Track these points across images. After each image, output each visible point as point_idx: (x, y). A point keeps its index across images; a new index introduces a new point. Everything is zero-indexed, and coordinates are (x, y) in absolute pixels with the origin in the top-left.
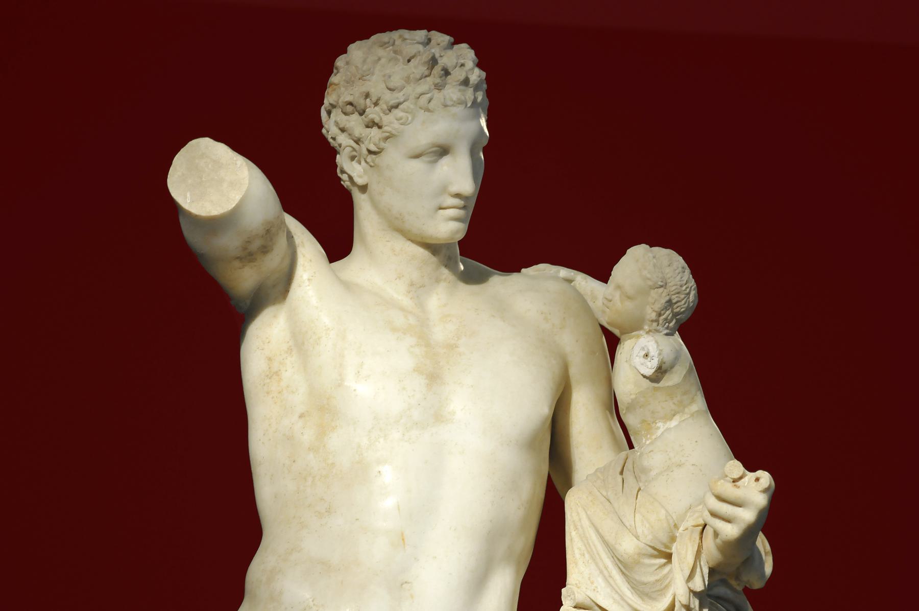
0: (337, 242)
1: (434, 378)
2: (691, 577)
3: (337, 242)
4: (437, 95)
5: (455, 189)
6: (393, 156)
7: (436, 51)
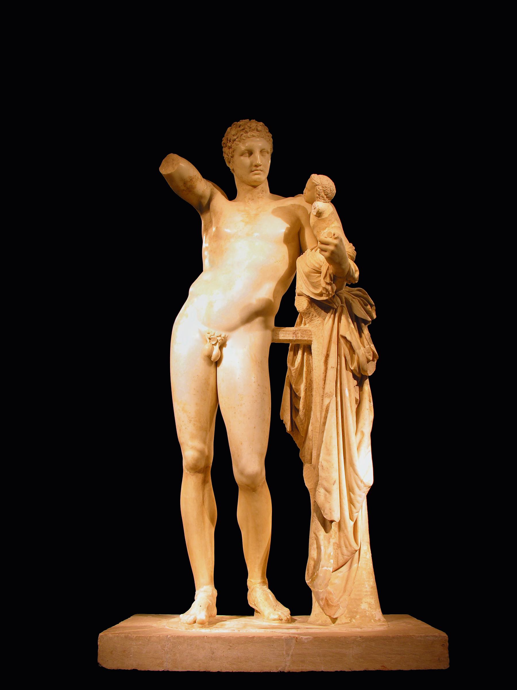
5: (254, 164)
6: (236, 156)
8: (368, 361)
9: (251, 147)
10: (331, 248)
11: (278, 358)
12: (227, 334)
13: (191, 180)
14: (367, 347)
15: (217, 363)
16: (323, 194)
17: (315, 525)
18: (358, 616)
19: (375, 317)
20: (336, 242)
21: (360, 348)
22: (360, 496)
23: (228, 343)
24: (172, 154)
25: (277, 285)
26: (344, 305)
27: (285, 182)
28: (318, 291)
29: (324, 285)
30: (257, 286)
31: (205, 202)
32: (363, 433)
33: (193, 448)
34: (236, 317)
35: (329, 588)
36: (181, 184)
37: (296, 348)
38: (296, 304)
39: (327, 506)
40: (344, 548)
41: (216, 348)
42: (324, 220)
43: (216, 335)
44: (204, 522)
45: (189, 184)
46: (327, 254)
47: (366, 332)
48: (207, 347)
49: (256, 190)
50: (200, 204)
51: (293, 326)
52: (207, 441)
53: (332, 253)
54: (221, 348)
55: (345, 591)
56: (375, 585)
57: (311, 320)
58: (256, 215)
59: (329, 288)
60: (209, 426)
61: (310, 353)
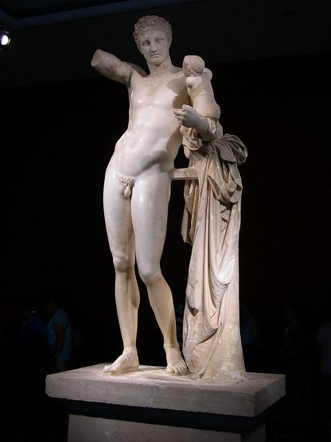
8: (231, 194)
9: (154, 37)
10: (182, 118)
12: (134, 178)
13: (112, 67)
14: (230, 181)
16: (192, 71)
17: (187, 310)
18: (218, 375)
20: (183, 113)
22: (218, 291)
25: (170, 139)
26: (215, 152)
30: (153, 142)
31: (127, 80)
32: (227, 245)
33: (116, 256)
34: (138, 166)
35: (196, 354)
36: (106, 71)
37: (190, 182)
39: (192, 297)
40: (206, 328)
41: (128, 188)
42: (194, 90)
44: (127, 303)
45: (111, 70)
48: (121, 187)
49: (159, 68)
50: (125, 81)
52: (127, 251)
53: (183, 121)
55: (207, 357)
58: (157, 88)
59: (195, 142)
60: (127, 240)
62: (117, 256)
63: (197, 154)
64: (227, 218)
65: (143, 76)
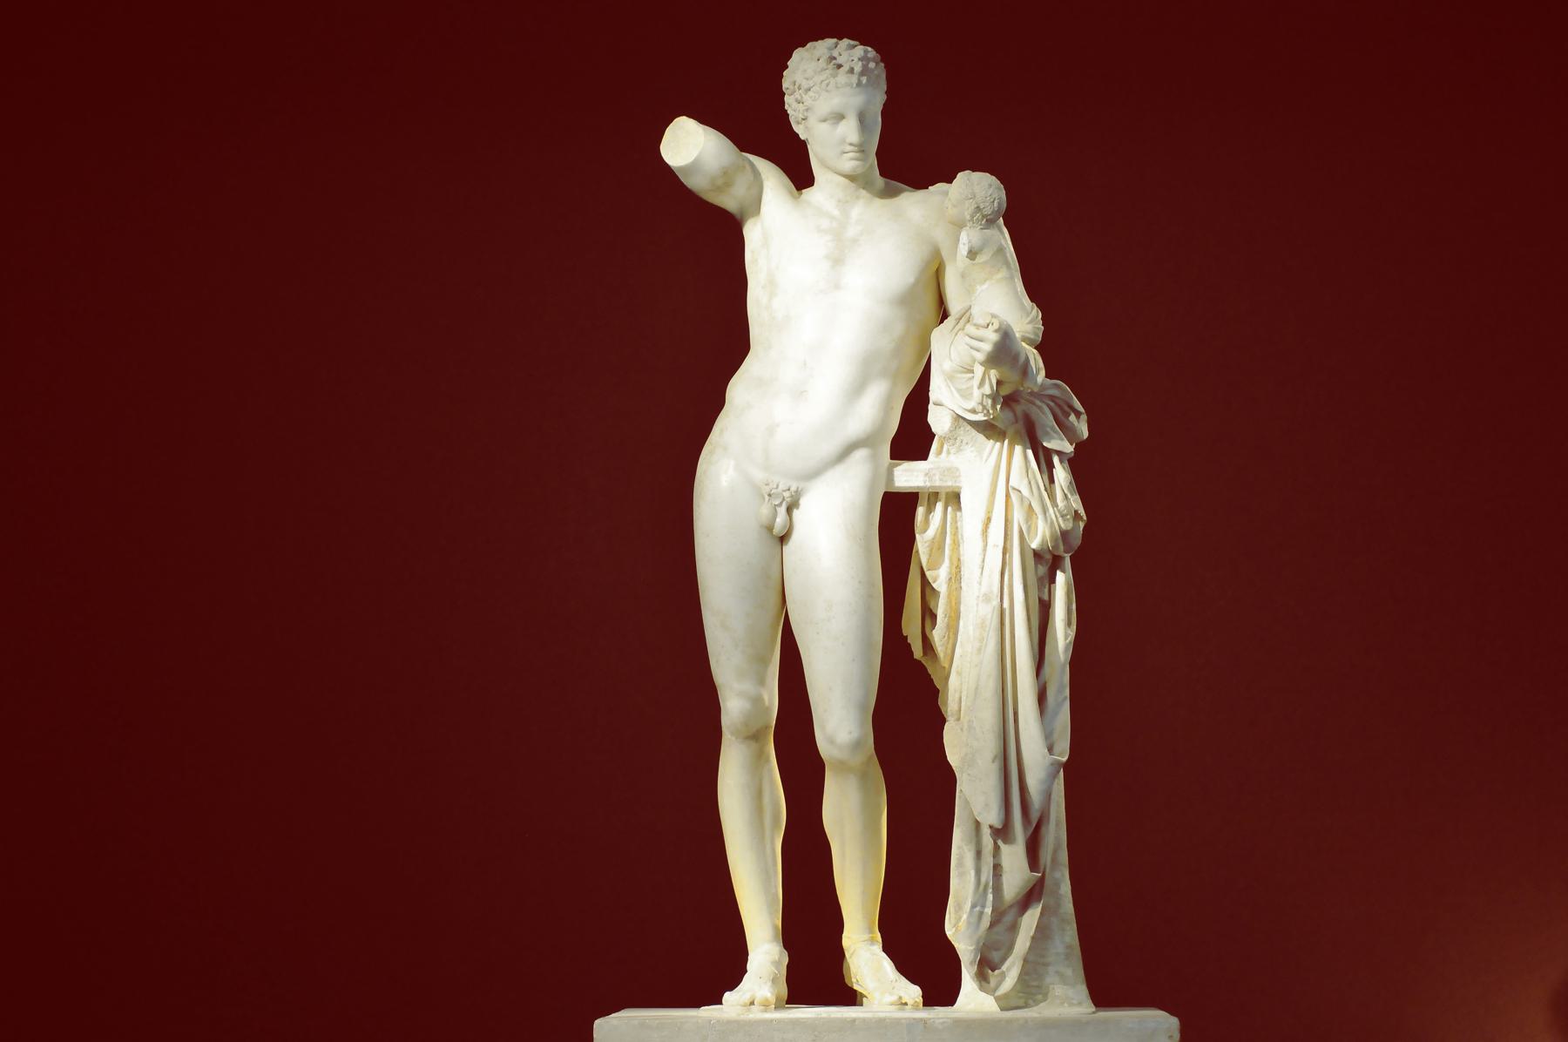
0: (801, 177)
1: (837, 261)
2: (981, 384)
3: (801, 177)
4: (832, 81)
6: (812, 121)
7: (835, 54)
10: (987, 347)
11: (897, 518)
15: (783, 539)
19: (1086, 434)
21: (1045, 511)
23: (802, 501)
24: (684, 118)
27: (908, 155)
28: (971, 404)
29: (977, 394)
30: (857, 389)
37: (934, 497)
38: (931, 419)
41: (782, 511)
43: (781, 487)
46: (981, 357)
47: (1061, 474)
48: (765, 511)
51: (924, 457)
54: (789, 510)
56: (1076, 942)
57: (959, 450)
58: (855, 241)
61: (959, 509)
62: (743, 694)
63: (974, 432)
64: (1046, 597)
65: (795, 198)
